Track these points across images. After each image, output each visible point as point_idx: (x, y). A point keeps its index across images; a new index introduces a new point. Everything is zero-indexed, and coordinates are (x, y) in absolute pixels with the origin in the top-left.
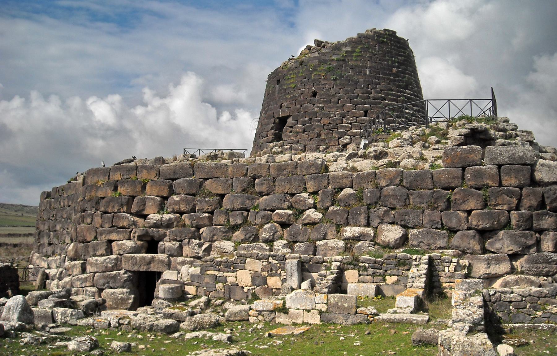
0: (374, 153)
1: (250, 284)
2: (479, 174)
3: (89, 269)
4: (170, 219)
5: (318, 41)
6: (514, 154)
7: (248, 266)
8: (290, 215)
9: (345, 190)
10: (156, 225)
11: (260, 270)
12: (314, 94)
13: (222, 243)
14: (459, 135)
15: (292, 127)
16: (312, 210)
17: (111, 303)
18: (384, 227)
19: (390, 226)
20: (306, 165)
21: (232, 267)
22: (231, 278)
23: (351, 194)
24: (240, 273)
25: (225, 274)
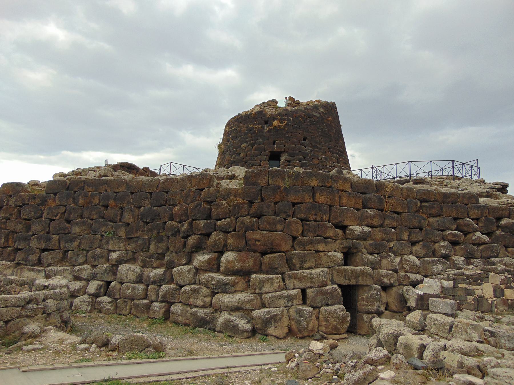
1: (493, 296)
3: (290, 283)
7: (490, 280)
12: (305, 139)
15: (289, 162)
17: (335, 323)
21: (478, 280)
22: (478, 290)
24: (485, 286)
25: (474, 287)
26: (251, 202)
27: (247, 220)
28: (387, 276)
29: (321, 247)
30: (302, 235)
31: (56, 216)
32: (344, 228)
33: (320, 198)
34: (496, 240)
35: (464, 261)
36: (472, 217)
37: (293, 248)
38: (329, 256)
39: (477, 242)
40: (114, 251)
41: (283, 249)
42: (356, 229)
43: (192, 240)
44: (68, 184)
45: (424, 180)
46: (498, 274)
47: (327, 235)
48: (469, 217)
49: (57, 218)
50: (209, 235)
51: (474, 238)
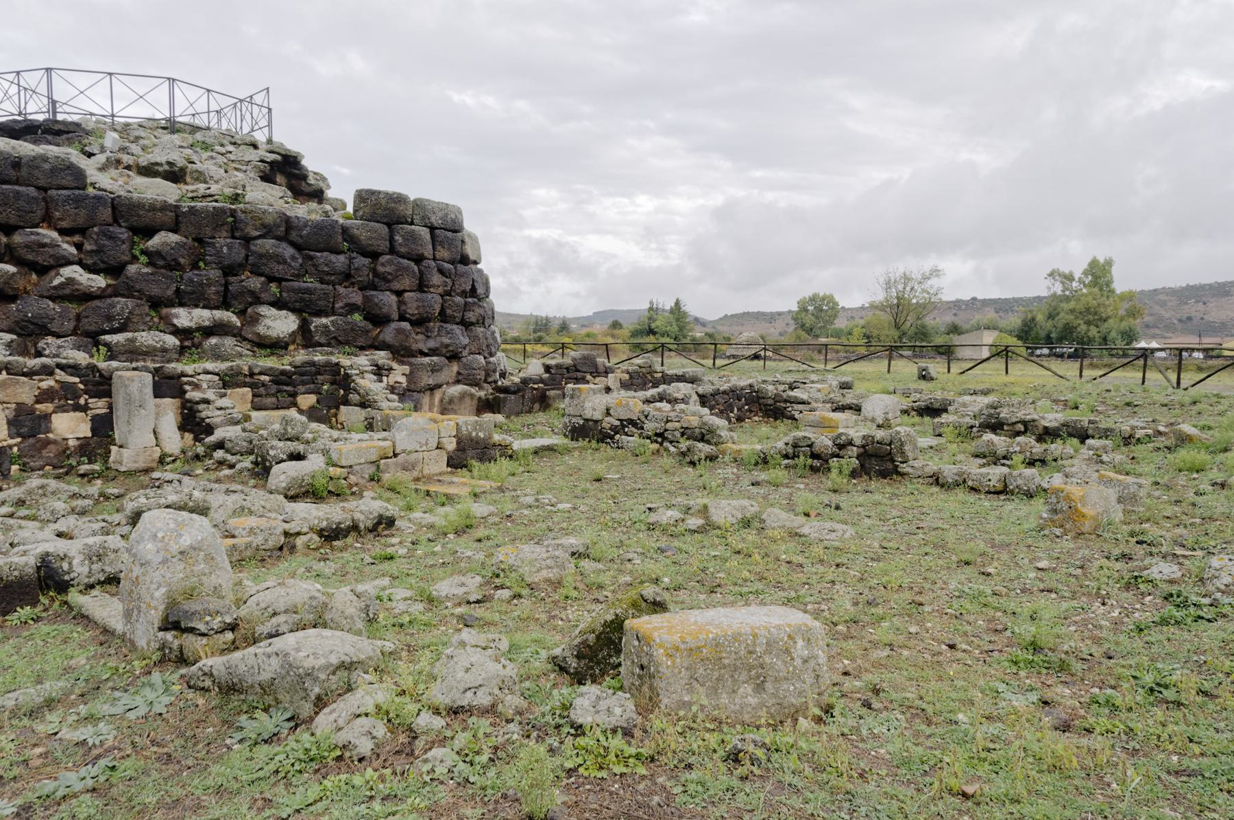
0: (167, 167)
2: (413, 237)
8: (14, 274)
9: (163, 233)
14: (262, 161)
16: (77, 268)
18: (264, 310)
19: (273, 311)
20: (47, 166)
23: (183, 245)
34: (128, 290)
35: (9, 345)
39: (67, 291)
45: (77, 125)
46: (24, 375)
51: (56, 282)
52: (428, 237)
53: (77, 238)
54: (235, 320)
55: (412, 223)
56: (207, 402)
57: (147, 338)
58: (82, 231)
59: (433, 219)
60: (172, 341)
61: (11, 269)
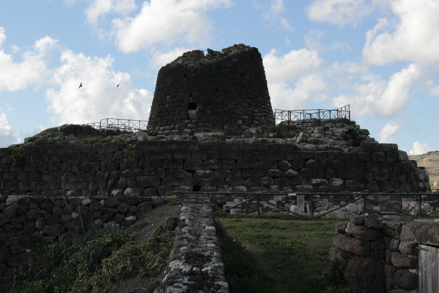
4: (210, 173)
5: (211, 50)
6: (391, 147)
10: (202, 177)
11: (281, 200)
12: (217, 90)
13: (240, 187)
15: (203, 111)
16: (291, 170)
26: (139, 160)
27: (137, 170)
28: (220, 198)
29: (176, 184)
30: (166, 177)
31: (32, 169)
32: (194, 172)
33: (177, 156)
36: (289, 159)
37: (160, 185)
38: (180, 188)
40: (69, 190)
41: (155, 186)
42: (200, 172)
43: (110, 182)
44: (37, 148)
47: (180, 177)
48: (287, 160)
49: (33, 171)
50: (119, 179)
52: (384, 155)
53: (292, 162)
54: (326, 181)
55: (378, 151)
56: (317, 202)
57: (305, 186)
58: (293, 161)
59: (386, 149)
60: (311, 187)
61: (278, 171)
